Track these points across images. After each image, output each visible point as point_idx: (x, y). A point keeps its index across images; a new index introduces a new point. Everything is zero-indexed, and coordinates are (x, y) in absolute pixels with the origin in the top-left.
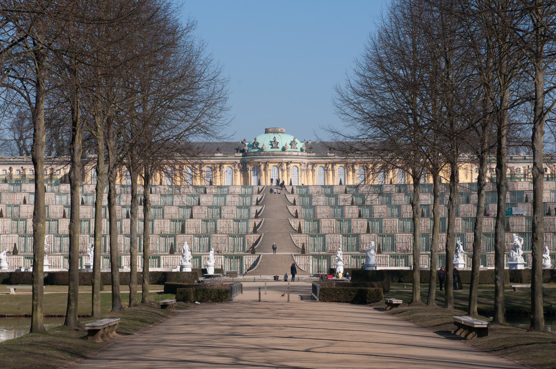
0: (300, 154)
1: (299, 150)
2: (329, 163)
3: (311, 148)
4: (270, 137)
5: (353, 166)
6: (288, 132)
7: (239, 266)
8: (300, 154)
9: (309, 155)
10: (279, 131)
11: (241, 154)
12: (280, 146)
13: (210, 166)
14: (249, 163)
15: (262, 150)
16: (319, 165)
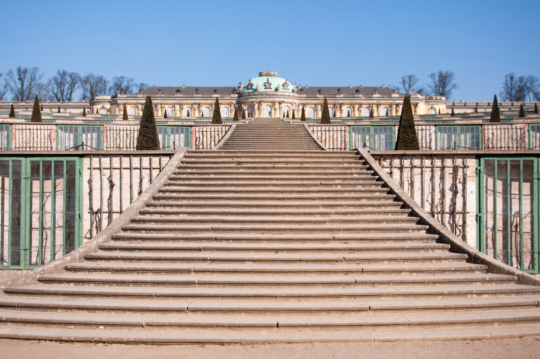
0: (292, 94)
1: (290, 91)
2: (319, 104)
3: (301, 90)
4: (264, 79)
5: (341, 107)
6: (280, 76)
7: (60, 221)
8: (292, 94)
9: (299, 96)
10: (272, 74)
11: (237, 95)
12: (273, 87)
13: (208, 106)
14: (244, 103)
15: (256, 90)
16: (309, 106)
